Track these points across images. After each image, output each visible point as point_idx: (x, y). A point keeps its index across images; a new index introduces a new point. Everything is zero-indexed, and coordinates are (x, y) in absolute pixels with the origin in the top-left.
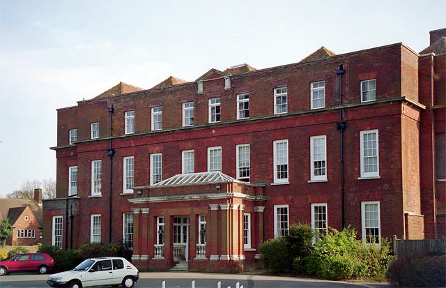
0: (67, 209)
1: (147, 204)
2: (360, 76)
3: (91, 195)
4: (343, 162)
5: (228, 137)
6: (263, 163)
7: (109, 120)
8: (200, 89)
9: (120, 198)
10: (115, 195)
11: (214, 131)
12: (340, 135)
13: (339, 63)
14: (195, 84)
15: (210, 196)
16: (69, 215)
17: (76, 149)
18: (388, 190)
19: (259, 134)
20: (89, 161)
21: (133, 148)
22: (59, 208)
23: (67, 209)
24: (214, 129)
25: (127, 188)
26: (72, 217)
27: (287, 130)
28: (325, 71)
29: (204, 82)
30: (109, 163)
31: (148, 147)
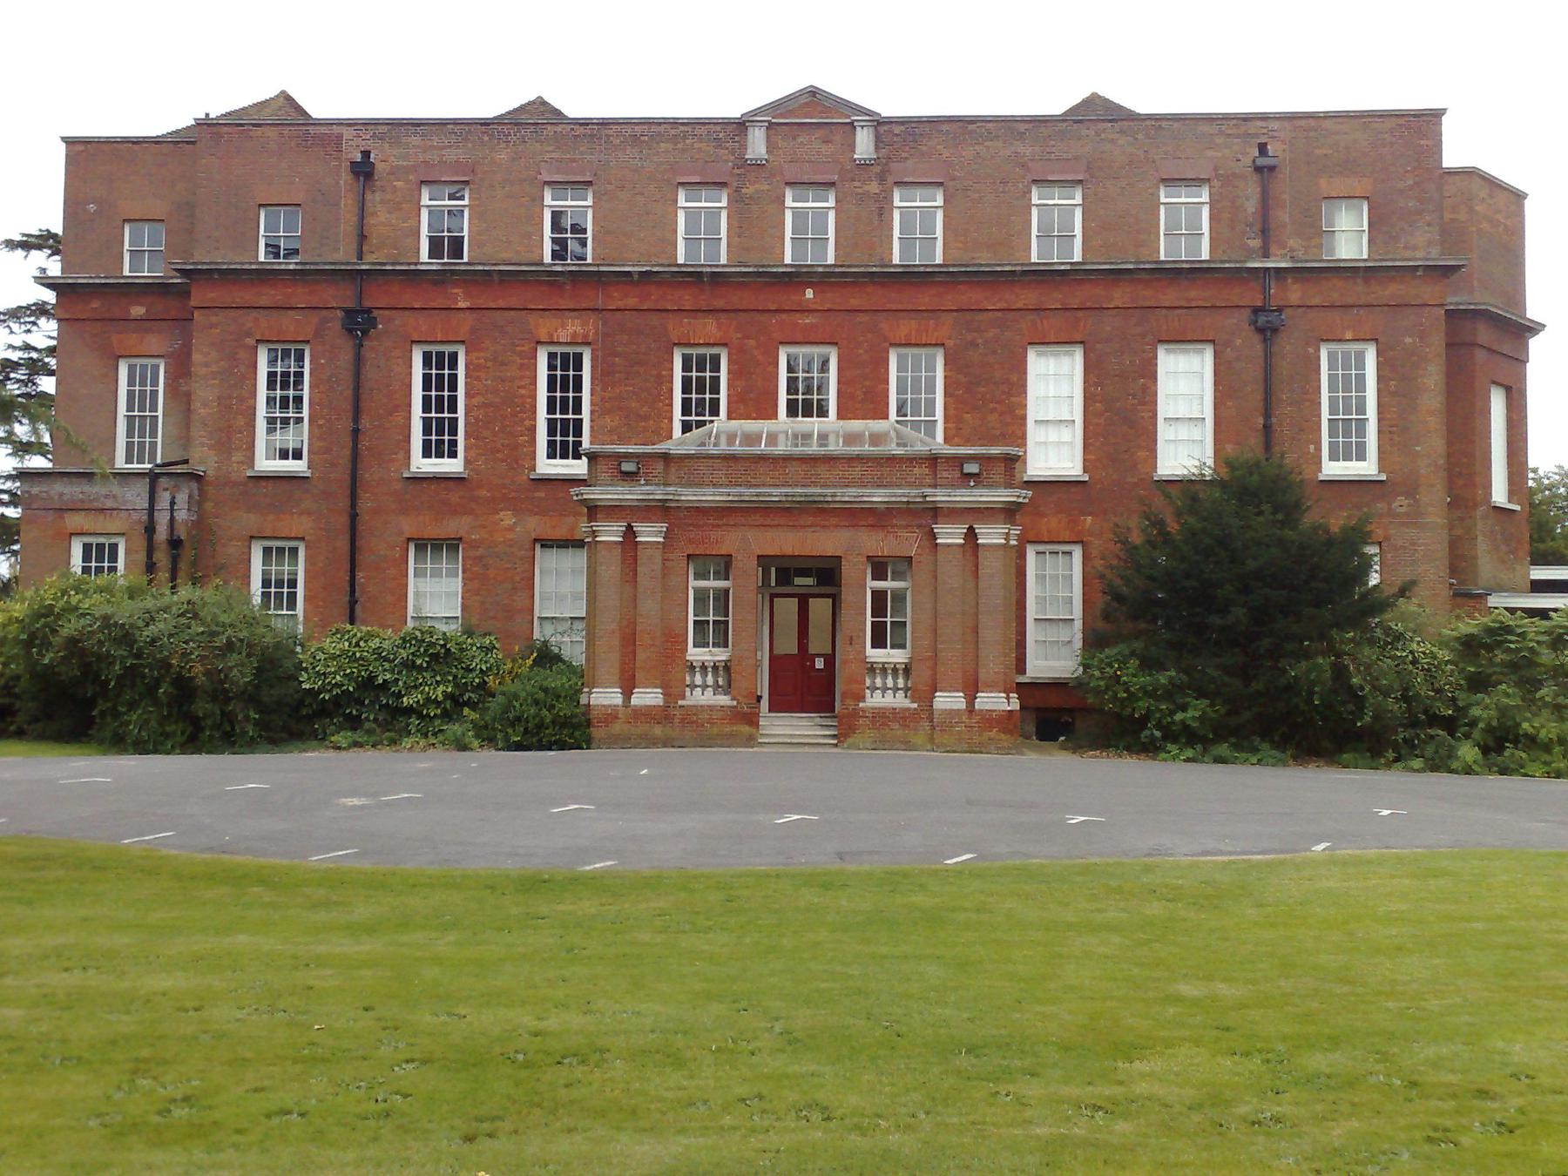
0: (151, 509)
1: (661, 510)
2: (1323, 182)
3: (408, 466)
4: (1267, 428)
5: (862, 318)
6: (992, 411)
7: (347, 205)
8: (757, 144)
9: (398, 486)
10: (369, 474)
11: (809, 294)
12: (1259, 347)
13: (1256, 135)
14: (740, 126)
15: (941, 496)
16: (162, 533)
17: (187, 294)
18: (1407, 514)
19: (980, 317)
20: (250, 341)
21: (461, 315)
22: (109, 504)
23: (151, 509)
24: (810, 285)
25: (551, 456)
26: (175, 543)
27: (1080, 314)
28: (1210, 153)
29: (771, 126)
30: (346, 357)
31: (532, 319)
